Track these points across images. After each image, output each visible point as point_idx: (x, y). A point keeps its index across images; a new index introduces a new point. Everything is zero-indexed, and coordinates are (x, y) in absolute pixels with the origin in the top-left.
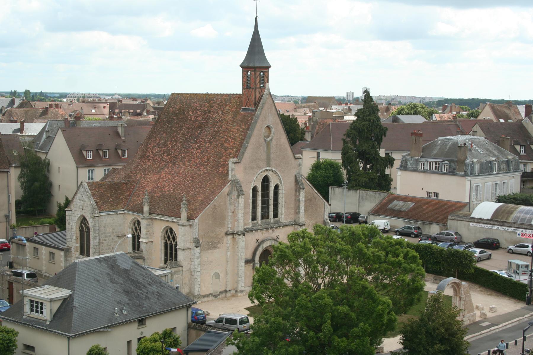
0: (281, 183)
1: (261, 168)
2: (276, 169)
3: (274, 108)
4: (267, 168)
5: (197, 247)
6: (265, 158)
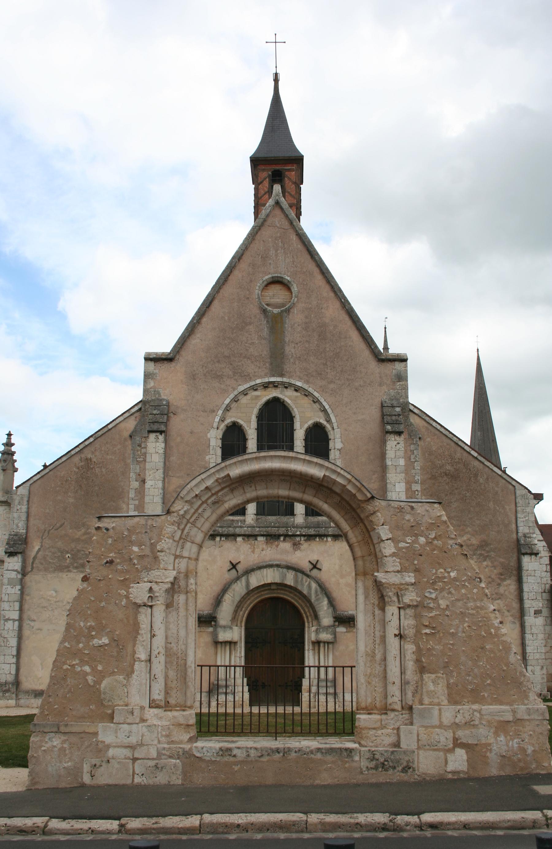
0: (329, 421)
1: (247, 377)
2: (307, 382)
3: (294, 237)
4: (272, 379)
5: (11, 554)
6: (266, 353)
